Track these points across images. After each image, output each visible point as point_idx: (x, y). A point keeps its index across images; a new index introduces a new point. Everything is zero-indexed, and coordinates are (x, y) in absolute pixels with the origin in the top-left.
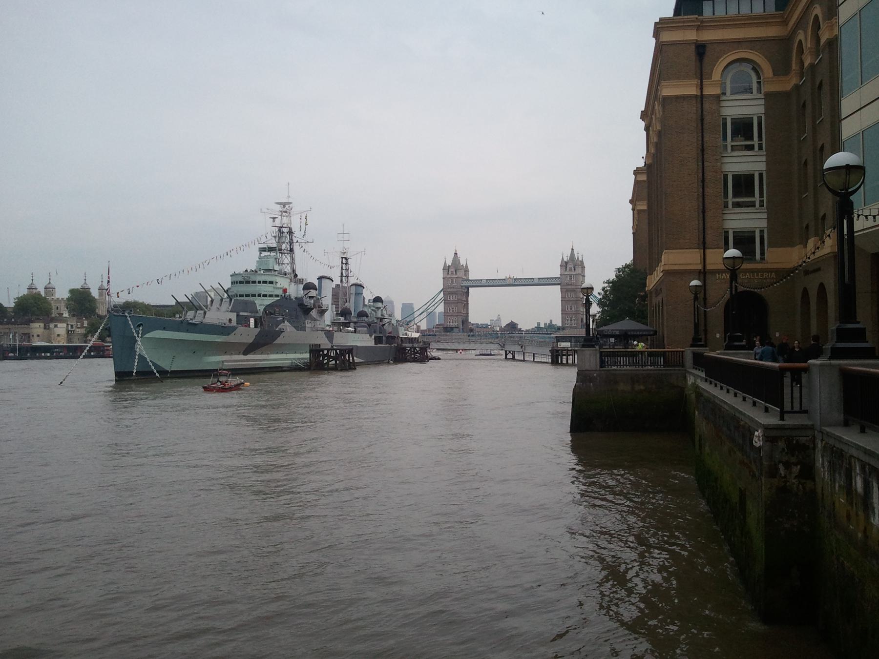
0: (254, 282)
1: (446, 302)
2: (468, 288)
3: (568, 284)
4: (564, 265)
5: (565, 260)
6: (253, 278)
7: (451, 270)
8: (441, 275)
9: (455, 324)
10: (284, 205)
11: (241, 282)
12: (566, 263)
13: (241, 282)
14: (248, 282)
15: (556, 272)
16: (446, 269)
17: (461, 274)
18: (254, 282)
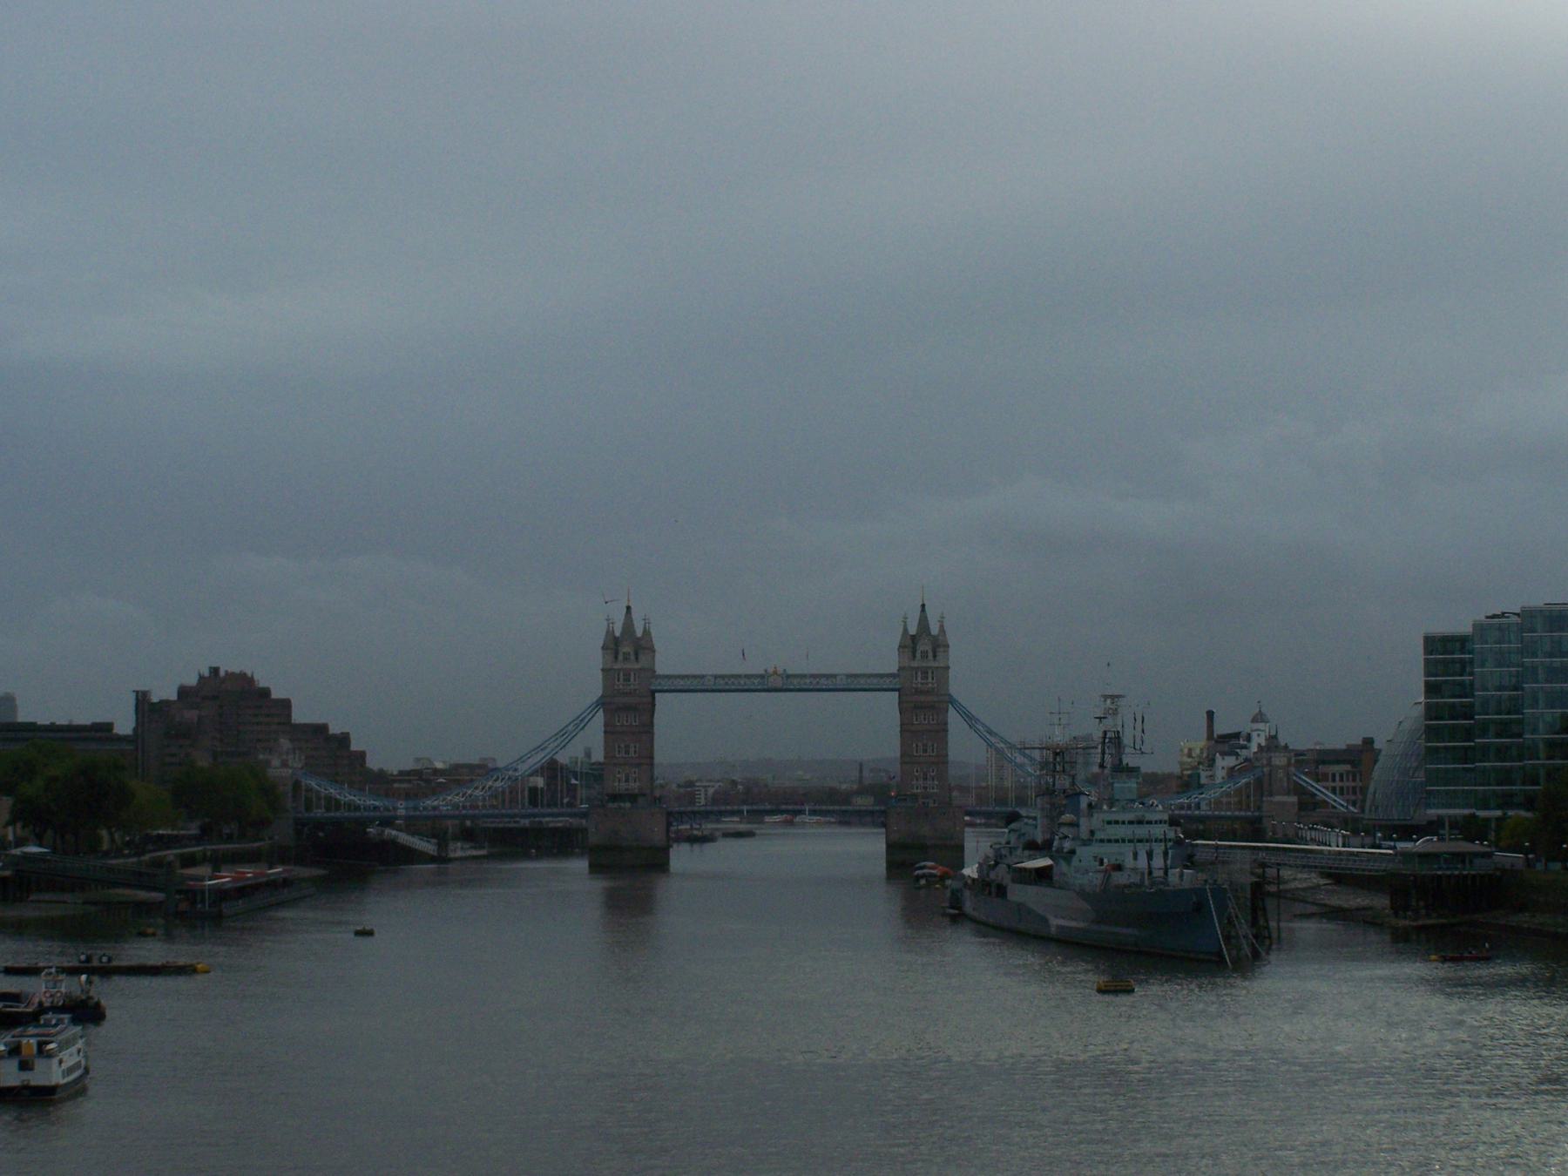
0: (1149, 822)
1: (609, 731)
2: (653, 693)
3: (918, 692)
4: (910, 644)
5: (913, 630)
6: (1149, 817)
7: (626, 648)
8: (595, 660)
9: (634, 786)
10: (1113, 697)
11: (1131, 822)
12: (913, 637)
13: (1131, 822)
14: (1140, 822)
15: (889, 661)
16: (613, 645)
17: (644, 662)
18: (1149, 822)
